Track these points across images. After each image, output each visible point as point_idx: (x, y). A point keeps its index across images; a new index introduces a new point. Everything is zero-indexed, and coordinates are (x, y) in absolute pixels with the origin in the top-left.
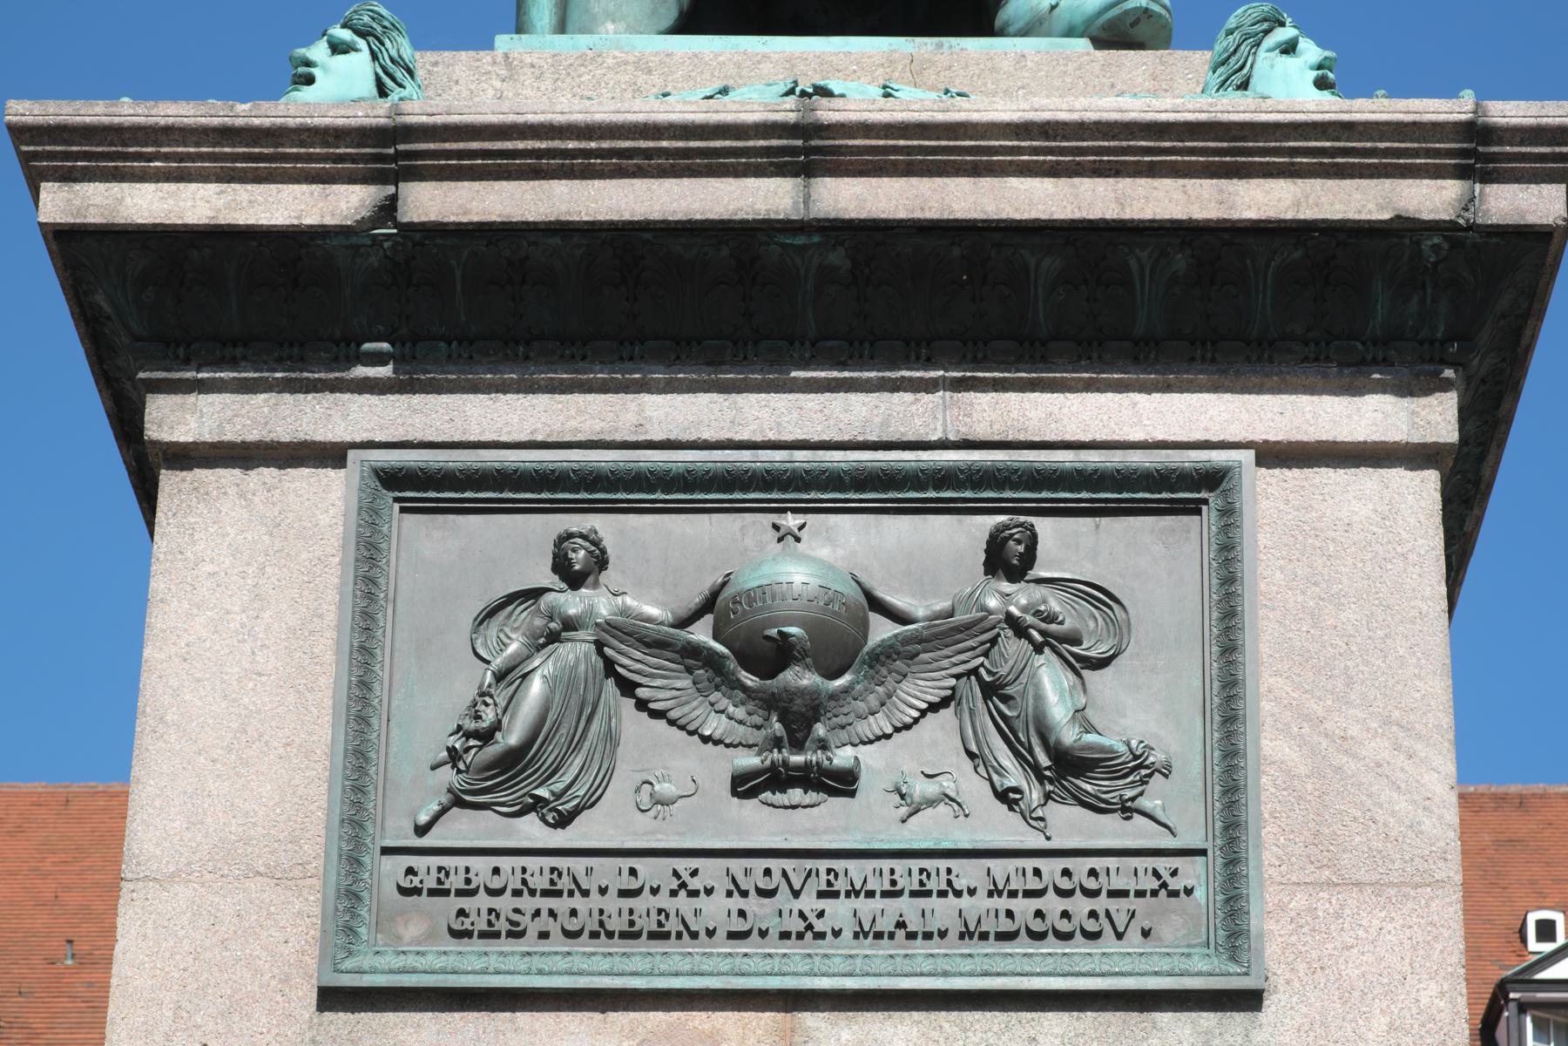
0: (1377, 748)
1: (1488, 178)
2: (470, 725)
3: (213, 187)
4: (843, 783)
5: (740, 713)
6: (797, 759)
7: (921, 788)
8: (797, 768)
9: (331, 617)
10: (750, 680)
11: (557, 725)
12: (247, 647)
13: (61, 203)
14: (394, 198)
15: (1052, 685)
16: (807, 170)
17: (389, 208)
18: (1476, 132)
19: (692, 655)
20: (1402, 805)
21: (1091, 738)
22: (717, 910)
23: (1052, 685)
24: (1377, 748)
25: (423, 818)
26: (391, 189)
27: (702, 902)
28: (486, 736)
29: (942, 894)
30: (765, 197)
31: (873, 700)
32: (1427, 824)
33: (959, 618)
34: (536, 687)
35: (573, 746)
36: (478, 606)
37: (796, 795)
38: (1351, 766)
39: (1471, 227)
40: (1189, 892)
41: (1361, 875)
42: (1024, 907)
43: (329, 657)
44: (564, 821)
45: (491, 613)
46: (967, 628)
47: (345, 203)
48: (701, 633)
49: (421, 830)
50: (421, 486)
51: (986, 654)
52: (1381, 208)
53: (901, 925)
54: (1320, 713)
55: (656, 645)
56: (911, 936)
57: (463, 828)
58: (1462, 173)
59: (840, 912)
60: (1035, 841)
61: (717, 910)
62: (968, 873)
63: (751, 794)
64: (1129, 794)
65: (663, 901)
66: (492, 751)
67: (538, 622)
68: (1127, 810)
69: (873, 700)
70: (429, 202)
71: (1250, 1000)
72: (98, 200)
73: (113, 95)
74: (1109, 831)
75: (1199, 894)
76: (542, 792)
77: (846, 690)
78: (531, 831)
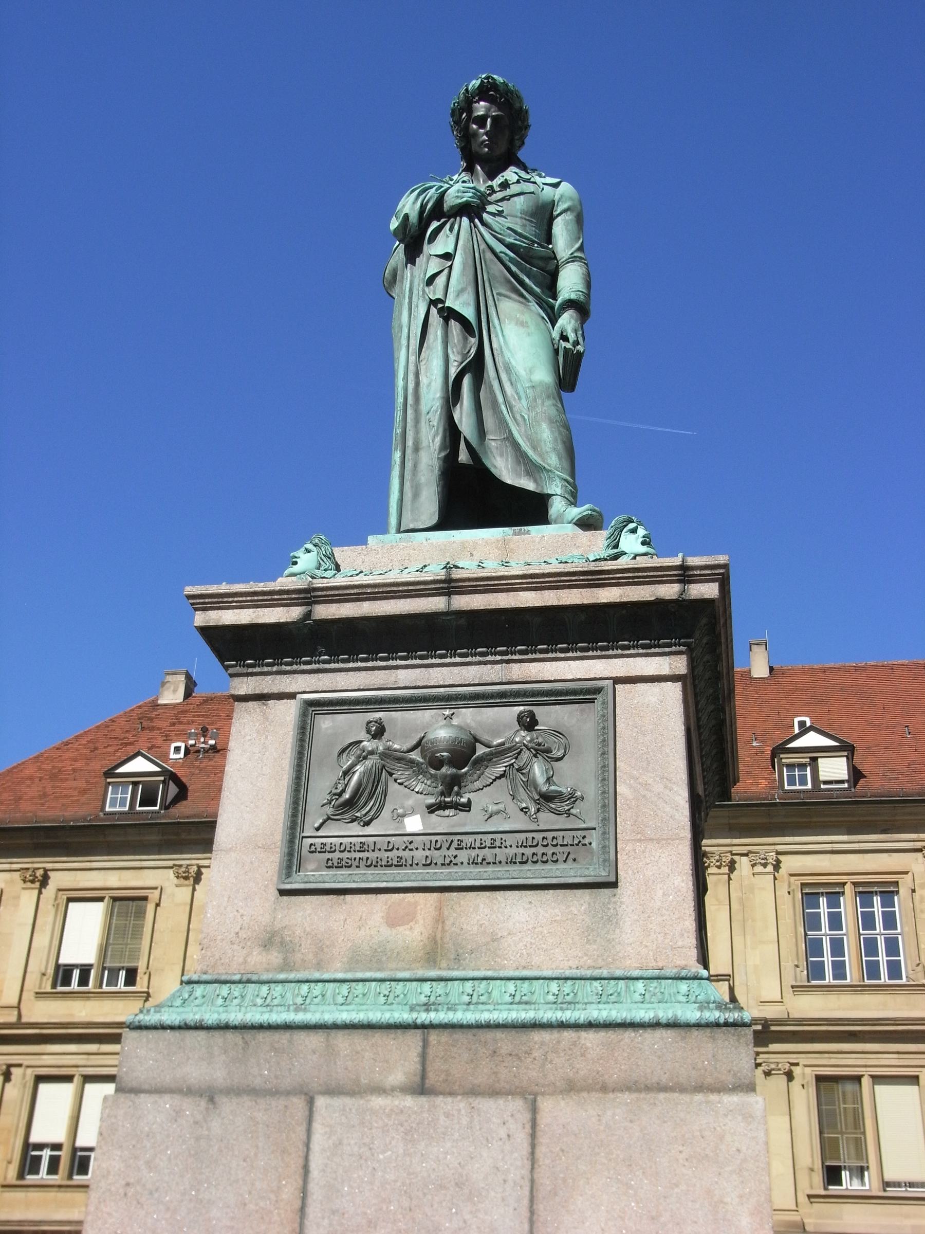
0: (658, 788)
1: (690, 582)
2: (334, 791)
3: (251, 610)
4: (467, 807)
5: (429, 782)
6: (448, 799)
7: (492, 808)
8: (448, 803)
9: (289, 754)
10: (433, 772)
11: (364, 790)
12: (260, 766)
13: (200, 619)
14: (311, 611)
15: (538, 770)
16: (449, 594)
17: (308, 615)
18: (684, 568)
19: (412, 762)
20: (668, 809)
21: (553, 788)
22: (419, 855)
23: (538, 770)
24: (658, 788)
25: (316, 825)
26: (310, 608)
27: (415, 853)
28: (340, 795)
29: (500, 847)
30: (437, 604)
31: (475, 776)
32: (677, 816)
33: (507, 745)
34: (356, 778)
35: (370, 797)
36: (339, 748)
37: (447, 812)
38: (649, 794)
39: (684, 600)
40: (590, 844)
41: (652, 836)
42: (529, 851)
43: (287, 768)
44: (367, 824)
45: (343, 750)
46: (509, 749)
47: (293, 614)
48: (415, 756)
49: (318, 829)
50: (314, 708)
51: (516, 758)
52: (651, 596)
53: (483, 860)
54: (638, 775)
55: (399, 760)
56: (489, 863)
57: (332, 829)
58: (678, 581)
59: (463, 856)
60: (534, 827)
61: (419, 855)
62: (510, 839)
63: (432, 812)
64: (567, 808)
65: (400, 853)
66: (342, 800)
67: (359, 752)
68: (568, 814)
69: (475, 776)
70: (324, 612)
71: (614, 885)
72: (214, 617)
73: (219, 583)
74: (561, 822)
75: (594, 845)
76: (358, 814)
77: (466, 773)
78: (355, 829)
